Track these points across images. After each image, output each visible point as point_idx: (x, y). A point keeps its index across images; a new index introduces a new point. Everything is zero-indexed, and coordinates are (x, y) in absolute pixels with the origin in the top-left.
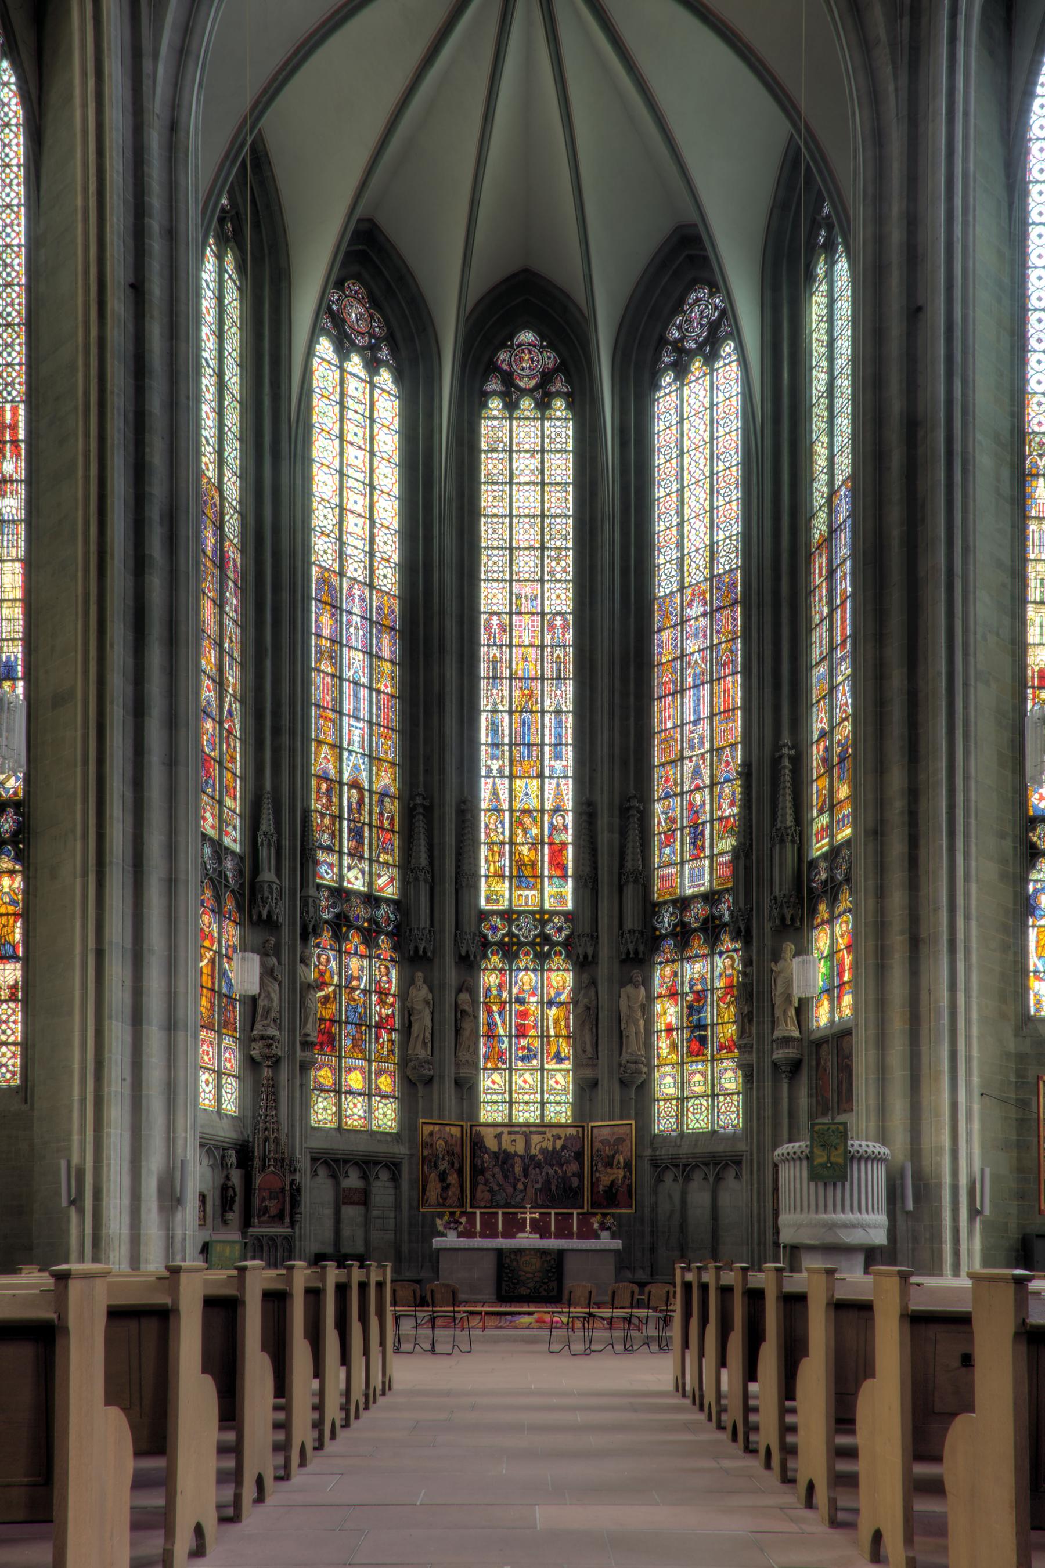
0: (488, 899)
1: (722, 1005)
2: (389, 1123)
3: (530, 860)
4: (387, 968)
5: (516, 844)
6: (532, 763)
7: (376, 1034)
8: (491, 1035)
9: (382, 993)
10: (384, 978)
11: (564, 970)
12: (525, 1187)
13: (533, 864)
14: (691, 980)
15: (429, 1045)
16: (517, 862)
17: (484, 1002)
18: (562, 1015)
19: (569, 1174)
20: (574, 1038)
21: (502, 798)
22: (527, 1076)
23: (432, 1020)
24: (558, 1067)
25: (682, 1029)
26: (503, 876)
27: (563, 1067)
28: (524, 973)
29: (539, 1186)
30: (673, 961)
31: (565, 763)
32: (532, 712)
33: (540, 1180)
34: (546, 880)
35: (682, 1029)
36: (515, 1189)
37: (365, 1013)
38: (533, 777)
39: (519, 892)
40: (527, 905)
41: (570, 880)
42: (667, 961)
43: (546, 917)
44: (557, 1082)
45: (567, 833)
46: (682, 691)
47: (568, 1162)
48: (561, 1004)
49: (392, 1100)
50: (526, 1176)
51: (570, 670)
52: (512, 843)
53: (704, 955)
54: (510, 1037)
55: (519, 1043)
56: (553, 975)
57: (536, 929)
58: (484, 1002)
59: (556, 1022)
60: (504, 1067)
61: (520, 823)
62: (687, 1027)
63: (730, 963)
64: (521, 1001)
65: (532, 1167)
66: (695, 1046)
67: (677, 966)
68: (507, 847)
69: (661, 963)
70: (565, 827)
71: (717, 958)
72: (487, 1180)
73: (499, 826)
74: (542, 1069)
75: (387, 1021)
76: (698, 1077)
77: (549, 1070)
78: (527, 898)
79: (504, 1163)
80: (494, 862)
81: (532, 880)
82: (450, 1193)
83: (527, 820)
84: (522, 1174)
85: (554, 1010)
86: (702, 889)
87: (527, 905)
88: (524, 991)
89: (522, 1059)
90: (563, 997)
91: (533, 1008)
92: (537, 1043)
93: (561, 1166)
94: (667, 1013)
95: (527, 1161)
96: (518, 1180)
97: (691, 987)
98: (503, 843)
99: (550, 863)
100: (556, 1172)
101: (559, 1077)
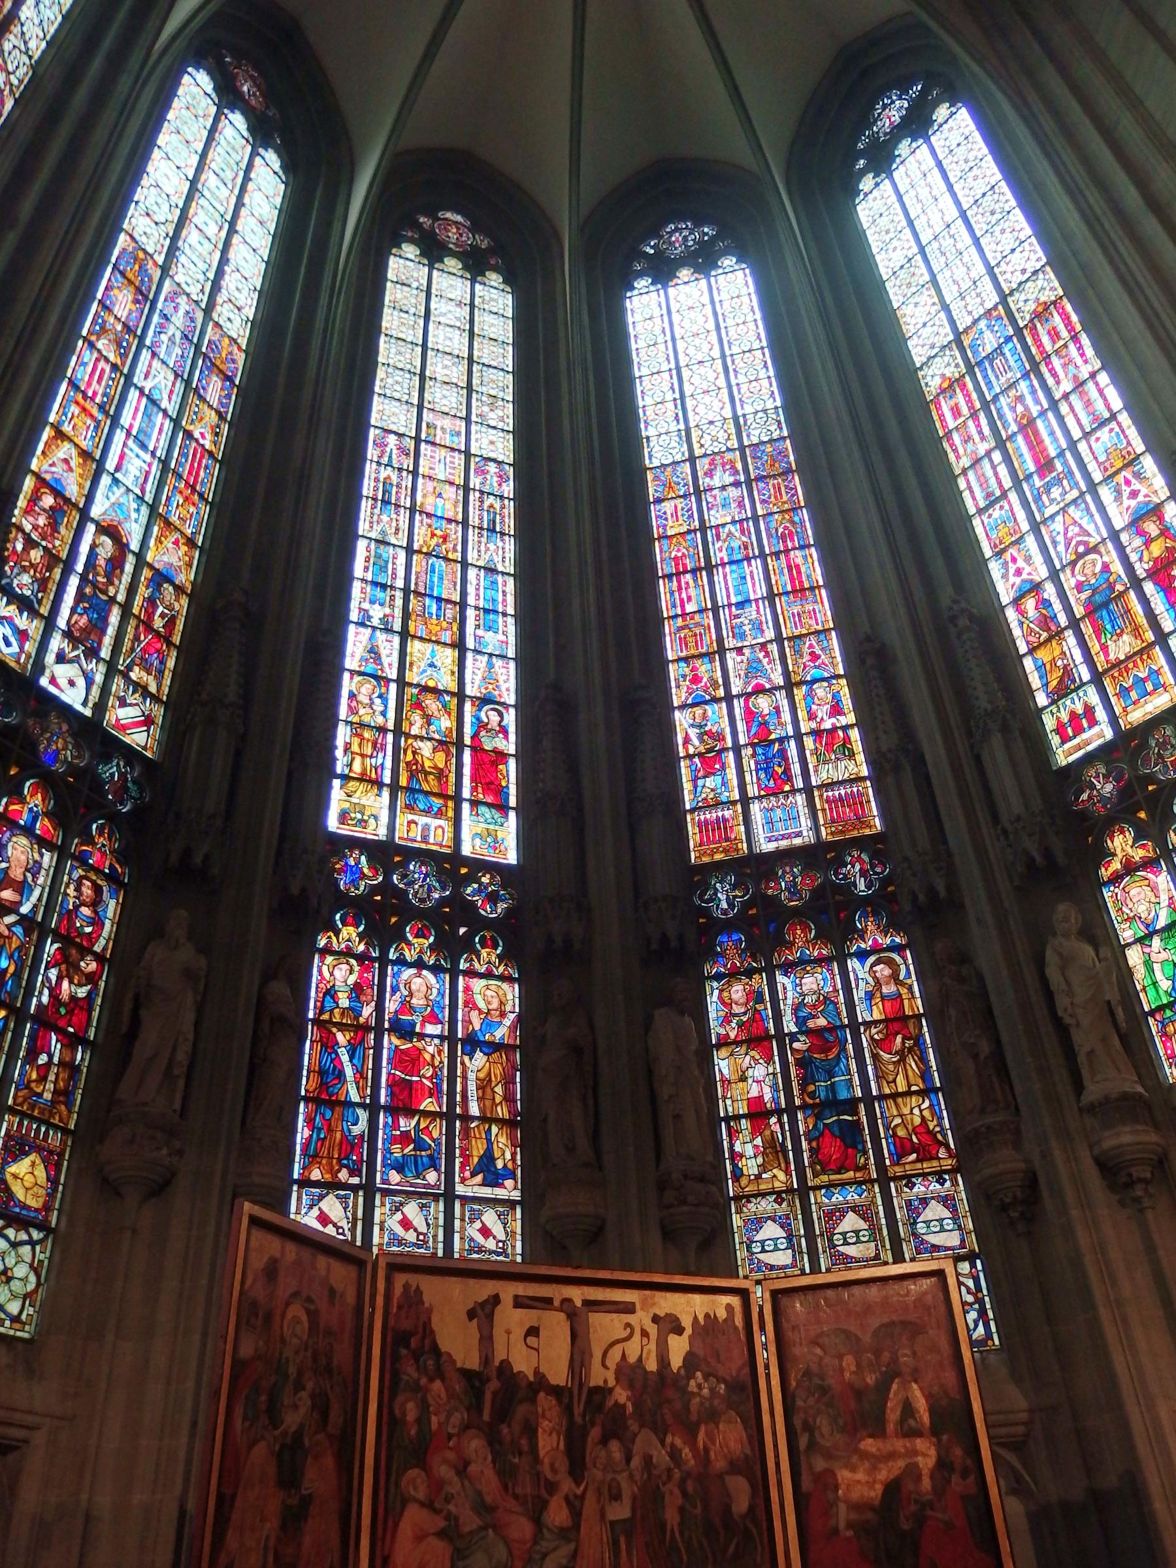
0: (343, 817)
1: (886, 1056)
2: (14, 1308)
3: (435, 767)
4: (97, 890)
5: (408, 736)
6: (444, 625)
7: (33, 1038)
8: (327, 1098)
9: (74, 946)
10: (85, 911)
11: (502, 978)
12: (576, 1514)
13: (441, 774)
14: (796, 1009)
15: (181, 1083)
16: (408, 764)
17: (316, 1022)
18: (498, 1070)
19: (720, 1464)
20: (527, 1126)
21: (385, 661)
22: (411, 1210)
23: (197, 1024)
24: (487, 1192)
25: (791, 1110)
26: (378, 784)
27: (500, 1193)
28: (413, 971)
29: (620, 1511)
30: (750, 973)
31: (502, 637)
32: (446, 559)
33: (627, 1490)
34: (466, 807)
35: (791, 1110)
36: (537, 1522)
37: (17, 975)
38: (445, 644)
39: (411, 817)
40: (425, 839)
41: (512, 815)
42: (734, 975)
43: (464, 871)
44: (485, 1232)
45: (506, 737)
46: (710, 568)
47: (712, 1416)
48: (493, 1048)
49: (36, 1235)
50: (577, 1466)
51: (510, 525)
52: (398, 732)
53: (821, 961)
54: (373, 1108)
55: (396, 1126)
56: (478, 985)
57: (444, 889)
58: (316, 1022)
59: (484, 1085)
60: (355, 1180)
61: (418, 705)
62: (804, 1107)
63: (887, 972)
64: (404, 1031)
65: (595, 1433)
66: (833, 1149)
67: (760, 982)
68: (390, 737)
69: (718, 977)
70: (504, 731)
71: (853, 964)
72: (437, 1485)
73: (378, 701)
74: (449, 1196)
75: (70, 1012)
76: (851, 1222)
77: (465, 1200)
78: (426, 829)
79: (502, 1414)
80: (363, 756)
81: (437, 802)
82: (307, 1540)
83: (432, 704)
84: (563, 1464)
85: (480, 1059)
86: (797, 841)
87: (425, 839)
88: (411, 1010)
89: (400, 1169)
90: (500, 1033)
91: (431, 1049)
92: (438, 1130)
93: (691, 1433)
94: (747, 1079)
95: (578, 1410)
96: (552, 1487)
97: (800, 1022)
98: (382, 730)
99: (474, 779)
100: (674, 1454)
101: (490, 1218)
